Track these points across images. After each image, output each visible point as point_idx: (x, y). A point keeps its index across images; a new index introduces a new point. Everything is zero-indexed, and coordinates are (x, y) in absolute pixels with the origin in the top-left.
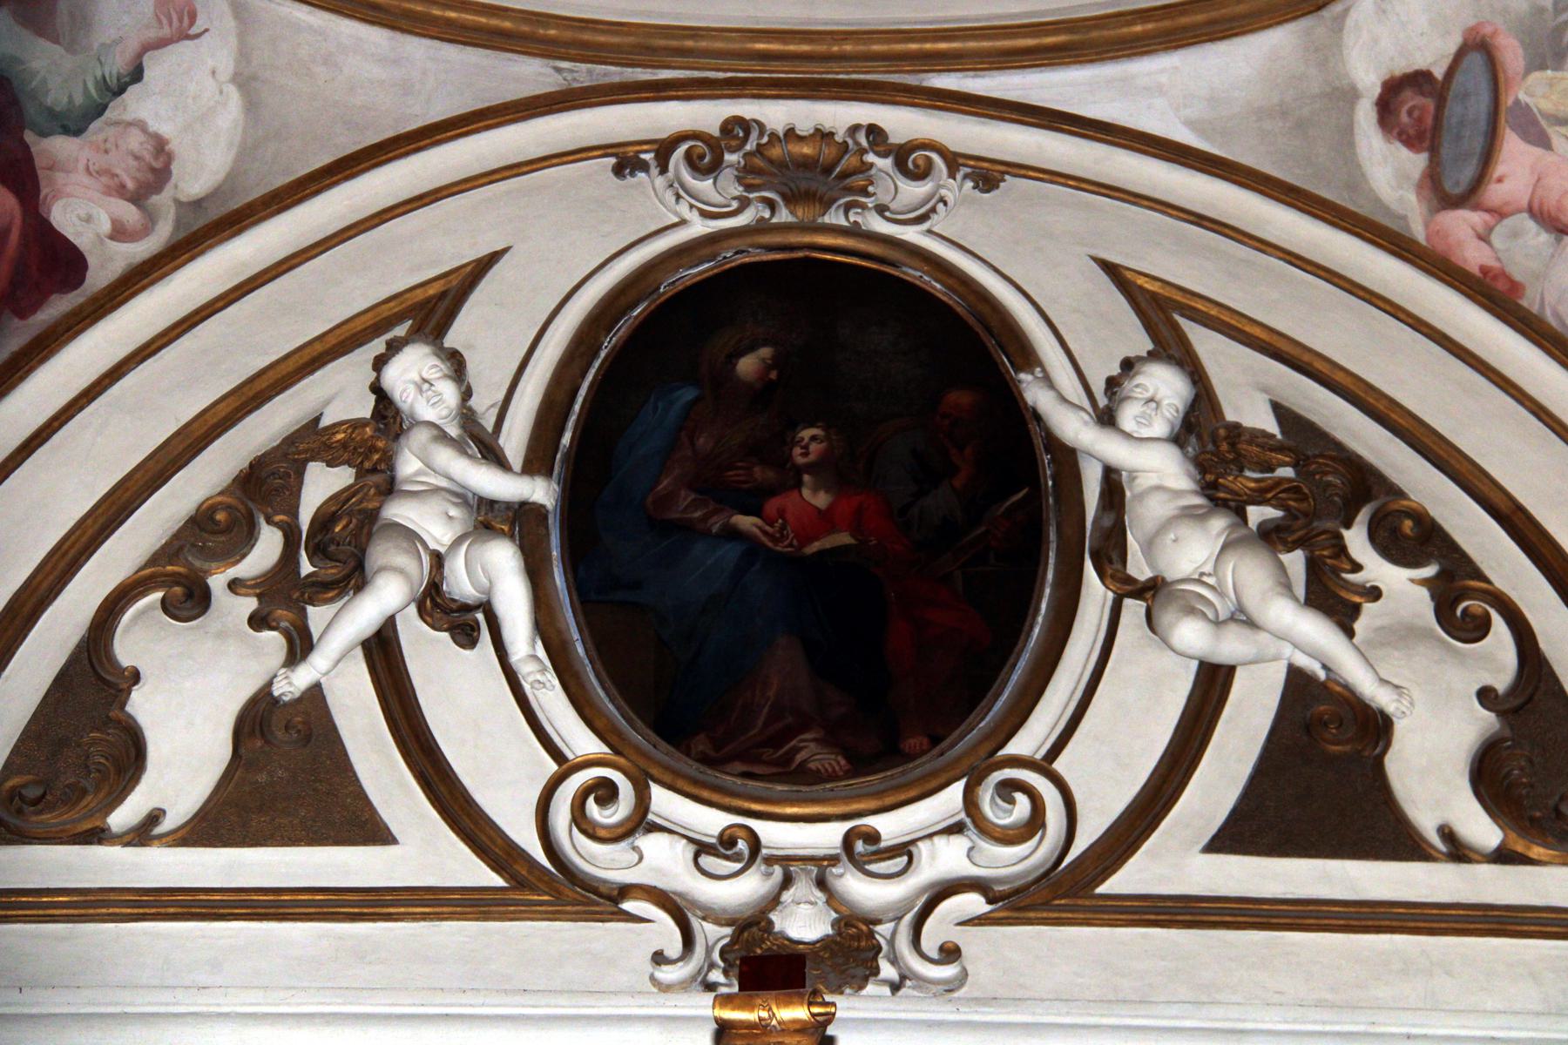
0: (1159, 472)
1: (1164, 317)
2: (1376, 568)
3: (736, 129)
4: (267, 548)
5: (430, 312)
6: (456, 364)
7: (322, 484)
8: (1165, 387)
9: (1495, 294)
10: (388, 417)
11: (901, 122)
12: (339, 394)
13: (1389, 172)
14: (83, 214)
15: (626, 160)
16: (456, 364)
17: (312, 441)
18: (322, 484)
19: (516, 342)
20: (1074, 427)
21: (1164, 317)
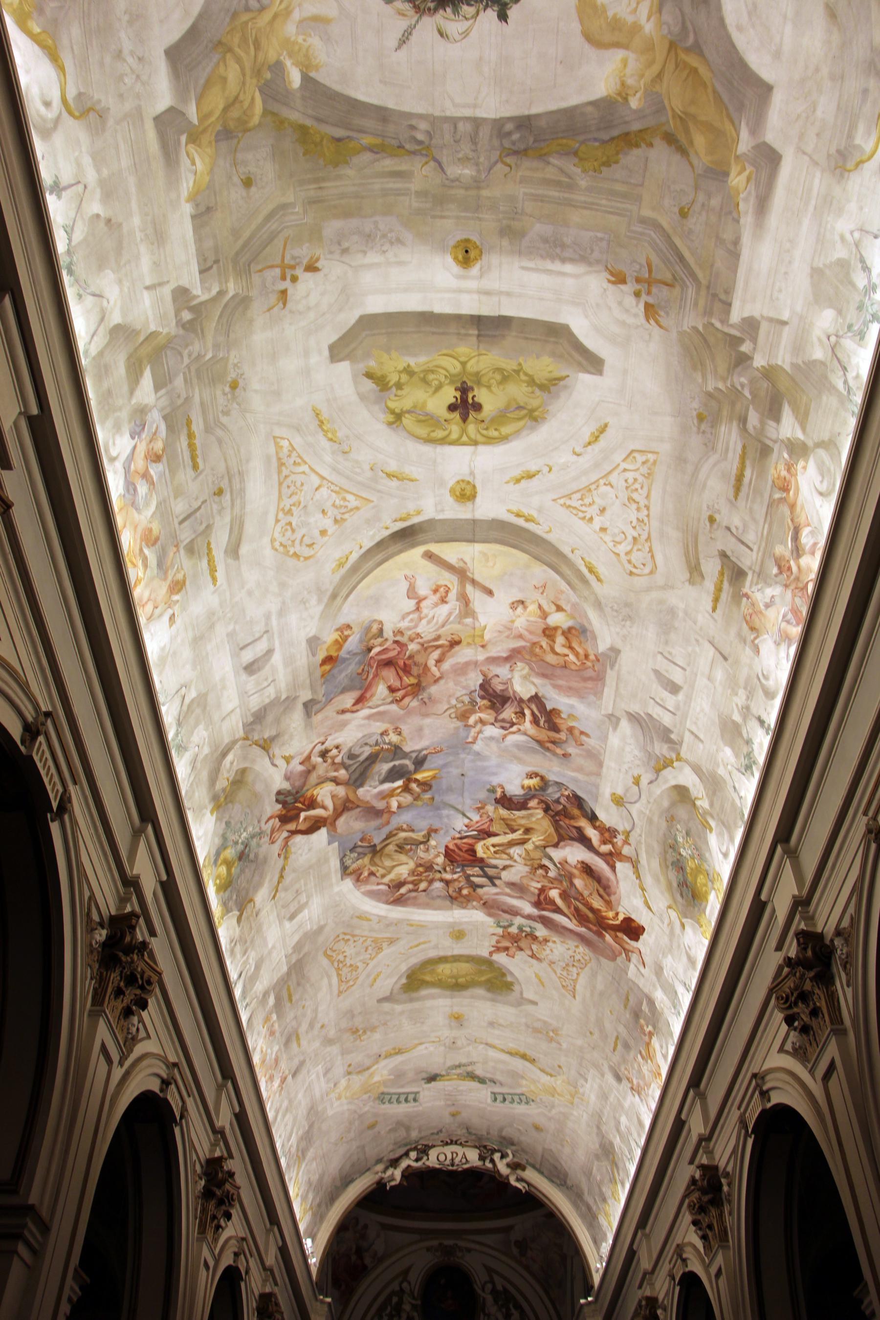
0: (489, 1299)
1: (489, 1270)
2: (513, 1311)
3: (440, 1244)
4: (389, 1308)
5: (406, 1272)
6: (409, 1283)
7: (395, 1300)
8: (489, 1286)
9: (527, 1268)
10: (402, 1290)
11: (461, 1243)
12: (395, 1286)
13: (515, 1251)
14: (368, 1261)
15: (428, 1249)
16: (409, 1283)
17: (393, 1293)
18: (395, 1300)
19: (416, 1278)
20: (480, 1292)
21: (489, 1270)
